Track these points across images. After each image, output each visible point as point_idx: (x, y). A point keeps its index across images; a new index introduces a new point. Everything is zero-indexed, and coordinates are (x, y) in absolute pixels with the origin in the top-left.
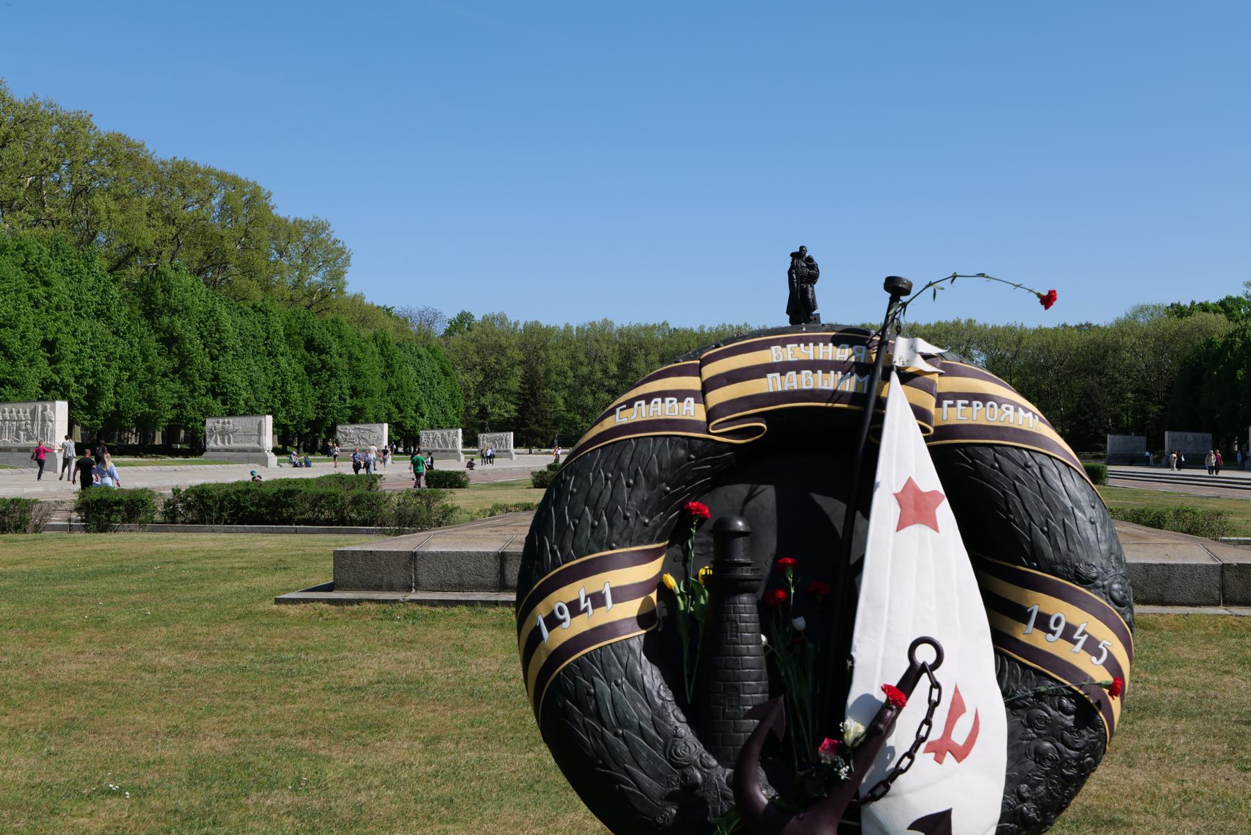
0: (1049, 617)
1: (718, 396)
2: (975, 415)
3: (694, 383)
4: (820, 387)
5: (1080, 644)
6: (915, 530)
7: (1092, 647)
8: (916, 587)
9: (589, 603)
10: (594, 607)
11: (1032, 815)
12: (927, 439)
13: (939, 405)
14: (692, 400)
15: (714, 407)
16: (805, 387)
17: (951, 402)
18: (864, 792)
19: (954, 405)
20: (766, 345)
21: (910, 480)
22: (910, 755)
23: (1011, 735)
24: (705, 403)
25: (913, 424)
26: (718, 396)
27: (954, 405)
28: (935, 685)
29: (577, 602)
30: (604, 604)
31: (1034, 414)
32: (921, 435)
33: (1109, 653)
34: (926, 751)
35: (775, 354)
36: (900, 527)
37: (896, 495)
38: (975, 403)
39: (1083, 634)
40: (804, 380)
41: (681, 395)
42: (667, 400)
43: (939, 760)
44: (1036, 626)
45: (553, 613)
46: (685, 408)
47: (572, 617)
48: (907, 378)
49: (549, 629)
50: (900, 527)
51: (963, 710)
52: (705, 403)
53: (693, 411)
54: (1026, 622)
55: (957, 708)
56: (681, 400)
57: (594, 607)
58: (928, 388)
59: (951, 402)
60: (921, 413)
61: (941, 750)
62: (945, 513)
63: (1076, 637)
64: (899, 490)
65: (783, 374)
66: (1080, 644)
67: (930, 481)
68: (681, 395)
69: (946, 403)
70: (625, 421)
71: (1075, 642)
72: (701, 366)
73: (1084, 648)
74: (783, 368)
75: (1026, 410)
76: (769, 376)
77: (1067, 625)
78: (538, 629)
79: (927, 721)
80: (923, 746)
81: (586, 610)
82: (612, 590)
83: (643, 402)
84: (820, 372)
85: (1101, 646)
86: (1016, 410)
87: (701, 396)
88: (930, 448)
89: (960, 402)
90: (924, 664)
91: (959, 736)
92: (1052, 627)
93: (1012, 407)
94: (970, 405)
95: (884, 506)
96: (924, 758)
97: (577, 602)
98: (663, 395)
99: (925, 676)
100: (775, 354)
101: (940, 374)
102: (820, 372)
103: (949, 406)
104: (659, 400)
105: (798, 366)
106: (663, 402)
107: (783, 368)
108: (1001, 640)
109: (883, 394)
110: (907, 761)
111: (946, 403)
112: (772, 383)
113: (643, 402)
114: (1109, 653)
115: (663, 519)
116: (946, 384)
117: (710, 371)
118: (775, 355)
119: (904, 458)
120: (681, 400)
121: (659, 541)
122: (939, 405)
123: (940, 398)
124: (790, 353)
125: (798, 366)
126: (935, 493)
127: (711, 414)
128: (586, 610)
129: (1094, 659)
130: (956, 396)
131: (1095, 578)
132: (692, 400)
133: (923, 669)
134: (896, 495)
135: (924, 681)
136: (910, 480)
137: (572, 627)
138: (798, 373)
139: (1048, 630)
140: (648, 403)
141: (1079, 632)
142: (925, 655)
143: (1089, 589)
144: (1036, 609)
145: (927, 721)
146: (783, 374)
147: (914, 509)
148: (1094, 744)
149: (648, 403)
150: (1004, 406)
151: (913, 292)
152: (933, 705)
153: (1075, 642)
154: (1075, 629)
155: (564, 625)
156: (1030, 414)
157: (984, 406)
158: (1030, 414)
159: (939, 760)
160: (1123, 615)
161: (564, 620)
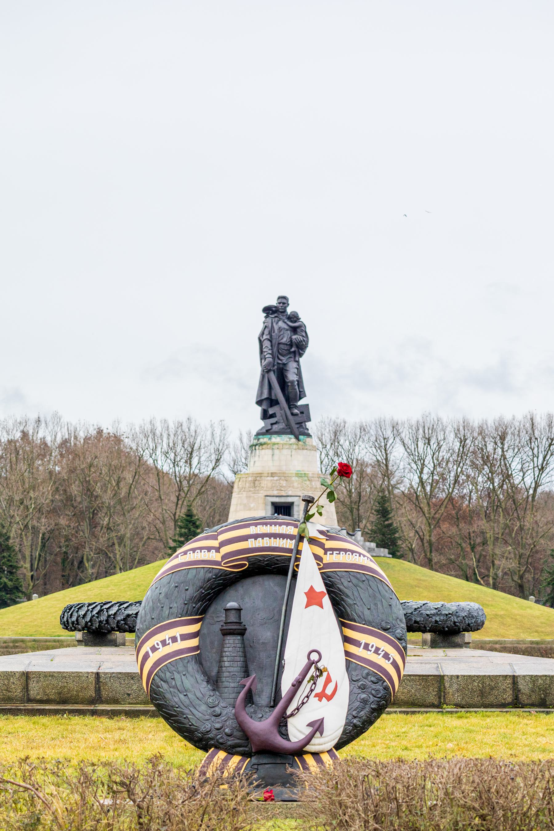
0: (369, 644)
1: (225, 550)
2: (342, 558)
4: (273, 545)
6: (315, 608)
7: (386, 656)
9: (170, 641)
10: (173, 642)
11: (358, 723)
12: (320, 569)
13: (325, 554)
14: (214, 551)
16: (265, 545)
17: (331, 552)
19: (333, 554)
20: (248, 526)
21: (312, 586)
22: (308, 697)
23: (351, 692)
25: (314, 562)
29: (165, 640)
30: (177, 641)
31: (368, 558)
32: (317, 567)
33: (393, 659)
34: (315, 697)
38: (341, 553)
39: (383, 651)
40: (265, 542)
41: (209, 549)
42: (203, 551)
43: (320, 700)
45: (154, 645)
46: (211, 555)
48: (312, 541)
49: (153, 652)
51: (331, 681)
53: (215, 556)
54: (360, 647)
55: (328, 680)
56: (209, 551)
57: (173, 642)
58: (322, 546)
60: (317, 558)
61: (321, 696)
62: (326, 601)
63: (379, 652)
64: (306, 591)
65: (256, 539)
67: (320, 587)
68: (209, 549)
69: (329, 553)
71: (379, 654)
72: (218, 535)
73: (383, 657)
74: (256, 537)
75: (364, 556)
77: (376, 647)
80: (314, 693)
81: (169, 644)
82: (180, 635)
83: (191, 552)
84: (272, 538)
85: (390, 656)
86: (360, 556)
87: (218, 550)
89: (335, 552)
91: (329, 691)
92: (370, 648)
93: (358, 555)
95: (300, 598)
97: (165, 640)
98: (201, 549)
101: (327, 540)
102: (272, 538)
103: (330, 554)
104: (199, 551)
105: (263, 536)
106: (201, 552)
107: (256, 537)
109: (299, 549)
110: (306, 699)
111: (329, 553)
113: (191, 552)
114: (393, 659)
115: (201, 605)
116: (329, 544)
117: (222, 538)
118: (252, 530)
119: (309, 576)
120: (209, 551)
121: (200, 615)
122: (325, 554)
123: (326, 551)
124: (259, 529)
125: (263, 536)
126: (323, 592)
127: (223, 557)
128: (169, 644)
129: (387, 661)
130: (332, 550)
131: (390, 628)
132: (214, 551)
136: (312, 586)
137: (163, 651)
138: (263, 539)
140: (194, 552)
141: (381, 650)
143: (387, 633)
146: (256, 539)
147: (313, 598)
148: (386, 696)
149: (194, 552)
151: (326, 493)
153: (379, 654)
154: (380, 649)
156: (366, 558)
158: (366, 558)
159: (320, 700)
160: (401, 644)
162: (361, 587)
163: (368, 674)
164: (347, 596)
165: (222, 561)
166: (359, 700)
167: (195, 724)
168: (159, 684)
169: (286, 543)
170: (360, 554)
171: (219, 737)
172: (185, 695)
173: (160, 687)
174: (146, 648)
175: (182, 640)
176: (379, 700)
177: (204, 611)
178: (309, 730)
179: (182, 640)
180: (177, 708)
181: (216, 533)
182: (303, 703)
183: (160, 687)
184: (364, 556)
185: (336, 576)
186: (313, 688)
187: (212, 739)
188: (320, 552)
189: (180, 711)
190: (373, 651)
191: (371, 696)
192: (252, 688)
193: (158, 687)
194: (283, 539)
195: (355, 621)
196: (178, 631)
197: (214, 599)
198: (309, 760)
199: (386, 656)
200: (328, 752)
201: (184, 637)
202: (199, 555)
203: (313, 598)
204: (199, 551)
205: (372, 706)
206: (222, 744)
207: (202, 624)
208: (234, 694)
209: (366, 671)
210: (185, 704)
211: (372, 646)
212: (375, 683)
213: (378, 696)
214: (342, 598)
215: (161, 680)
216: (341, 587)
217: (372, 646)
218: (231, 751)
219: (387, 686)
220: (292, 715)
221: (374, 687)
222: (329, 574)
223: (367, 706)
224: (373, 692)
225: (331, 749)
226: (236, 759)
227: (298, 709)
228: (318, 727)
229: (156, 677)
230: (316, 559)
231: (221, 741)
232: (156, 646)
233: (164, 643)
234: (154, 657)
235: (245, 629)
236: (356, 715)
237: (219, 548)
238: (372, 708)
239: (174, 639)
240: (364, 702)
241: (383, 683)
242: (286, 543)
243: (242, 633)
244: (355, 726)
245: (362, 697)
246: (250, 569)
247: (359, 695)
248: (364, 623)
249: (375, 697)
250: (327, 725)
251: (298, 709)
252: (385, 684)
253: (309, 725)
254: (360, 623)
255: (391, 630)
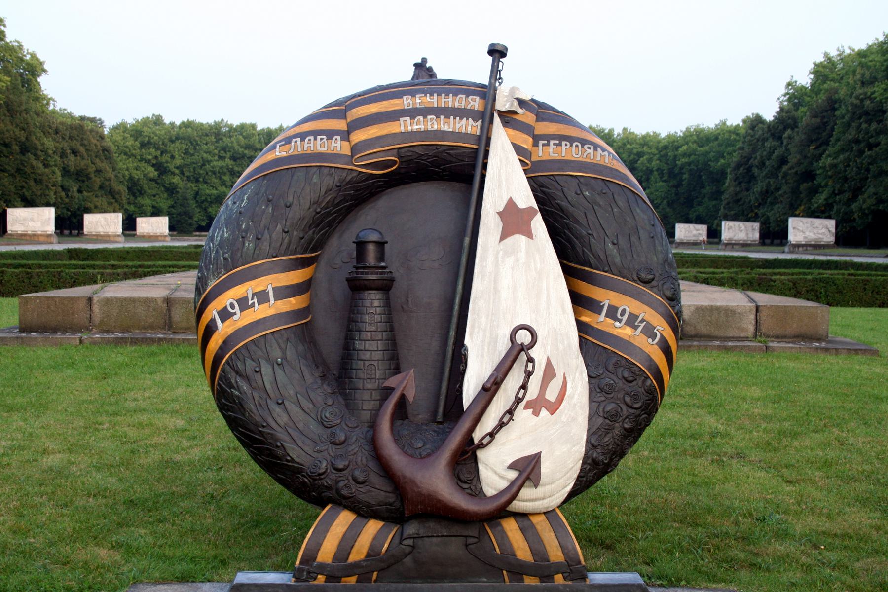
0: (617, 309)
1: (359, 136)
3: (340, 125)
5: (640, 329)
7: (649, 331)
8: (517, 287)
9: (255, 300)
11: (601, 458)
13: (535, 144)
15: (356, 144)
17: (545, 142)
18: (477, 435)
20: (399, 95)
22: (510, 412)
24: (349, 141)
25: (514, 158)
26: (359, 136)
27: (548, 144)
28: (531, 360)
30: (267, 300)
31: (609, 153)
35: (407, 102)
36: (503, 238)
37: (499, 213)
38: (564, 143)
39: (642, 320)
41: (330, 134)
42: (319, 137)
44: (606, 316)
45: (226, 308)
46: (333, 144)
47: (242, 310)
49: (223, 322)
50: (503, 238)
52: (349, 141)
53: (338, 146)
59: (545, 142)
64: (501, 210)
65: (413, 118)
66: (640, 329)
68: (330, 134)
69: (541, 142)
70: (284, 154)
72: (345, 111)
74: (413, 113)
75: (603, 150)
76: (402, 119)
77: (630, 314)
78: (213, 320)
79: (524, 387)
80: (522, 405)
82: (273, 288)
83: (299, 140)
86: (595, 149)
87: (346, 135)
88: (528, 178)
89: (552, 142)
90: (522, 344)
93: (592, 147)
94: (560, 145)
96: (522, 414)
99: (523, 353)
100: (407, 102)
103: (544, 145)
104: (312, 138)
105: (425, 112)
106: (315, 139)
107: (413, 113)
108: (581, 326)
110: (508, 416)
112: (405, 125)
113: (299, 140)
122: (535, 144)
123: (536, 139)
125: (425, 112)
127: (354, 149)
129: (650, 340)
130: (548, 137)
132: (339, 138)
133: (523, 348)
134: (498, 213)
135: (523, 357)
137: (241, 319)
138: (425, 117)
139: (616, 319)
142: (524, 337)
144: (606, 303)
145: (524, 387)
146: (413, 118)
149: (303, 140)
150: (586, 146)
152: (529, 374)
155: (235, 317)
157: (571, 145)
158: (606, 153)
161: (235, 314)
162: (600, 206)
163: (617, 365)
164: (577, 221)
165: (352, 156)
166: (601, 414)
167: (296, 459)
168: (233, 381)
169: (467, 125)
170: (596, 147)
171: (341, 484)
172: (278, 403)
173: (234, 388)
174: (212, 311)
175: (277, 298)
176: (638, 412)
177: (319, 245)
178: (513, 475)
179: (277, 298)
180: (264, 427)
181: (344, 107)
182: (501, 425)
183: (234, 388)
184: (603, 150)
185: (555, 183)
186: (520, 395)
187: (329, 488)
188: (526, 142)
189: (269, 433)
190: (623, 322)
191: (624, 407)
192: (405, 393)
193: (231, 386)
194: (461, 119)
195: (591, 267)
196: (268, 283)
197: (339, 223)
198: (510, 526)
199: (649, 331)
200: (544, 513)
201: (282, 293)
202: (312, 145)
203: (513, 221)
204: (312, 138)
205: (626, 426)
206: (345, 498)
207: (316, 268)
208: (373, 402)
209: (614, 360)
210: (279, 421)
211: (624, 311)
212: (631, 382)
213: (636, 406)
214: (566, 223)
215: (237, 373)
216: (564, 204)
217: (624, 311)
218: (365, 512)
219: (652, 385)
220: (481, 446)
221: (629, 390)
222: (540, 179)
223: (617, 424)
224: (628, 399)
225: (554, 510)
226: (373, 527)
227: (492, 435)
228: (528, 469)
229: (228, 368)
230: (518, 154)
231: (344, 492)
232: (230, 309)
233: (243, 303)
234: (224, 329)
235: (392, 280)
236: (596, 444)
237: (349, 133)
238: (625, 429)
239: (262, 297)
240: (613, 417)
241: (644, 381)
242: (467, 125)
243: (386, 286)
244: (595, 462)
245: (608, 408)
246: (403, 171)
247: (603, 404)
248: (606, 269)
249: (631, 407)
250: (545, 468)
251: (492, 435)
252: (648, 383)
253: (512, 467)
254: (599, 270)
255: (654, 283)
